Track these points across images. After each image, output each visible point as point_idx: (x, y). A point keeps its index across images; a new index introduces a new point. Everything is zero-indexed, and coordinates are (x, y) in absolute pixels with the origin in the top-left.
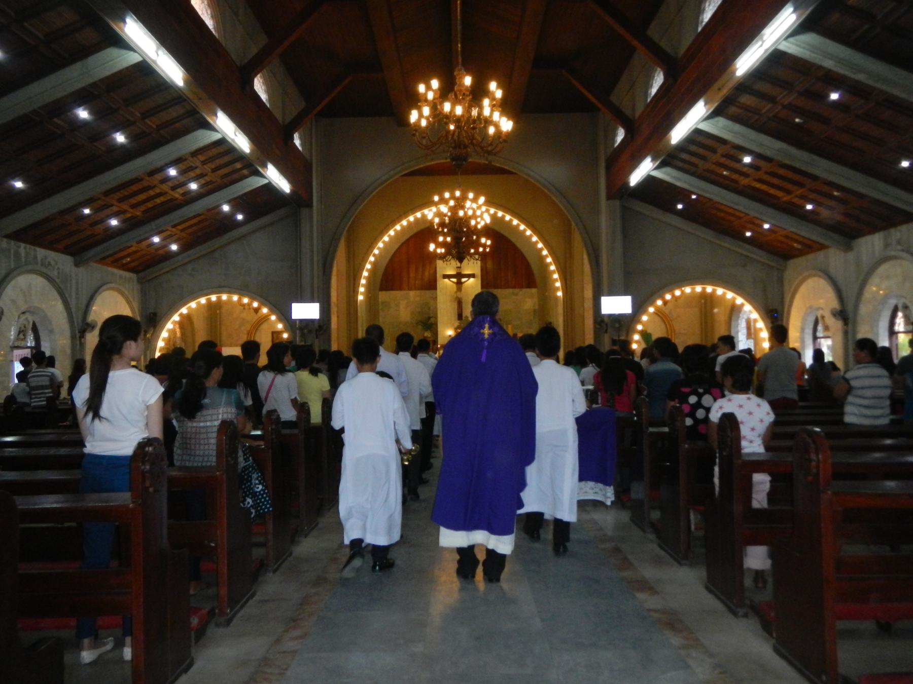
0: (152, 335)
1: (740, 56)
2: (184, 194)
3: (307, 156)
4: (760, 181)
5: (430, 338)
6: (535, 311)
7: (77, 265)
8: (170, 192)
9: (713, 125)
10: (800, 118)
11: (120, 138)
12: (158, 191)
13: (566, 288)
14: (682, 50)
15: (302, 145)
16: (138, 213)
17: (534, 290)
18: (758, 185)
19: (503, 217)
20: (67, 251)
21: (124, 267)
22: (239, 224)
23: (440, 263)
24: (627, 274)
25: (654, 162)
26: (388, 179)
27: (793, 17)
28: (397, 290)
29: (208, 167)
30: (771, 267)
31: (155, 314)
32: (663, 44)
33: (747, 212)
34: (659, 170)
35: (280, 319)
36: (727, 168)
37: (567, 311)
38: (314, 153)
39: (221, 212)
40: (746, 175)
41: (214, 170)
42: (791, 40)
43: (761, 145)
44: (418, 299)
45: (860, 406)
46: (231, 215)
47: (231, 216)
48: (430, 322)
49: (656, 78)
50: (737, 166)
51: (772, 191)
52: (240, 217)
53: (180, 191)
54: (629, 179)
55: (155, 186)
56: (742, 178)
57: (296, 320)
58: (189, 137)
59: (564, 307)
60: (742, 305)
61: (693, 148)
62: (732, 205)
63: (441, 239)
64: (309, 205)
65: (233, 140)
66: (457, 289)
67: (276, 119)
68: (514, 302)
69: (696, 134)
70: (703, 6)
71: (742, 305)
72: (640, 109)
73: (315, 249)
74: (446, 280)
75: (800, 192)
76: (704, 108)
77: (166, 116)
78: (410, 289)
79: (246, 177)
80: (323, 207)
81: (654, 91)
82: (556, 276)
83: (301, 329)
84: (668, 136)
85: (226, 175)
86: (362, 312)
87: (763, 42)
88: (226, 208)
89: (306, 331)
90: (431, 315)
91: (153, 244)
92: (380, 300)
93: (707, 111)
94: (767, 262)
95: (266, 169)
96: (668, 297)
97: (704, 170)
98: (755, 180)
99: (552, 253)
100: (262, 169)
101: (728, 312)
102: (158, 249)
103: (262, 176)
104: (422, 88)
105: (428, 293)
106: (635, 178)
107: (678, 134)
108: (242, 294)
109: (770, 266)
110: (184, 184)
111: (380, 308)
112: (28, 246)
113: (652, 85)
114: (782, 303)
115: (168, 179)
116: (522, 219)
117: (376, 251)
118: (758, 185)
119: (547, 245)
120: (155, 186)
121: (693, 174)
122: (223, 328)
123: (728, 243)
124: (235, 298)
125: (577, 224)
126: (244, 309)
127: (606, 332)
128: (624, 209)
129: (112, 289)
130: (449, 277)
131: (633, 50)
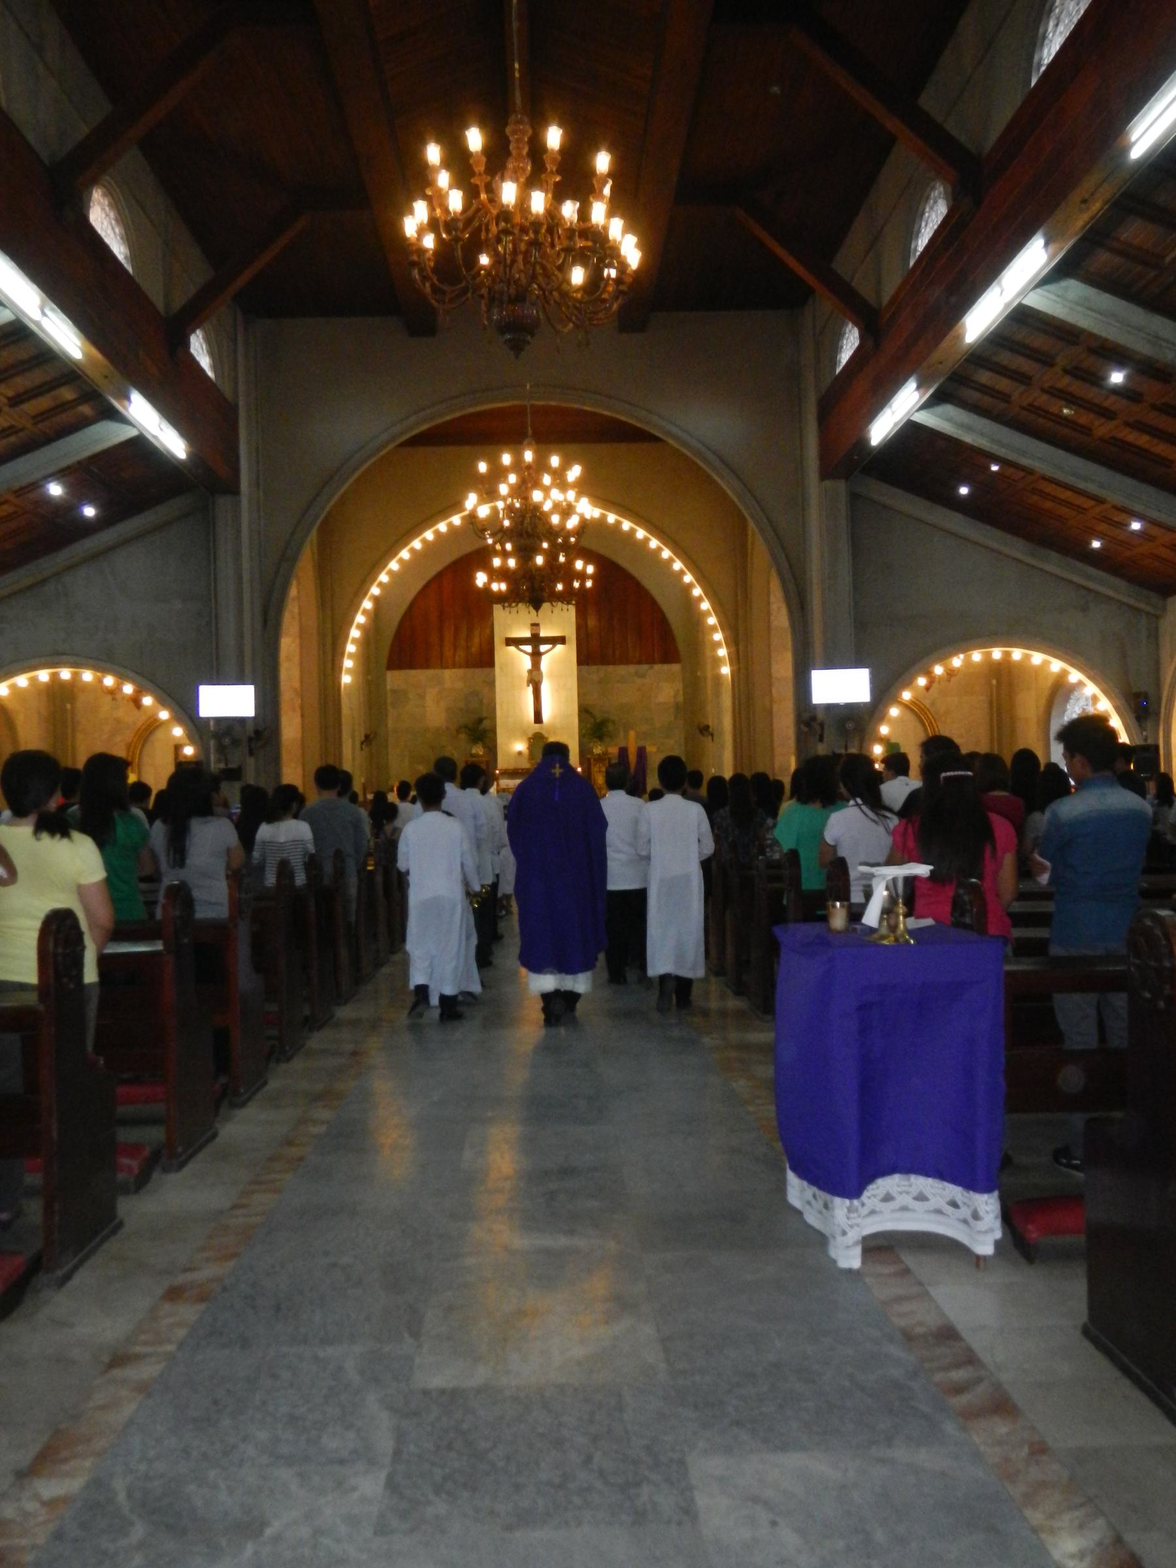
1: (1146, 107)
4: (1139, 426)
5: (481, 756)
6: (677, 706)
9: (1058, 296)
13: (737, 658)
14: (994, 135)
15: (214, 367)
17: (676, 668)
18: (1132, 437)
22: (89, 528)
23: (500, 614)
24: (861, 625)
25: (922, 390)
28: (421, 667)
30: (1138, 610)
32: (951, 127)
33: (1101, 493)
35: (177, 719)
37: (740, 704)
38: (242, 388)
39: (48, 500)
43: (1156, 339)
44: (459, 685)
47: (65, 511)
49: (927, 214)
50: (1091, 393)
52: (89, 512)
54: (869, 431)
56: (1103, 420)
57: (208, 719)
60: (1080, 684)
61: (1005, 358)
62: (1071, 480)
63: (497, 562)
64: (233, 489)
65: (38, 324)
67: (151, 303)
68: (639, 690)
69: (1021, 316)
70: (1041, 30)
71: (1080, 684)
72: (891, 285)
73: (246, 577)
74: (512, 649)
76: (1043, 251)
78: (443, 665)
80: (261, 494)
81: (922, 242)
82: (718, 636)
83: (218, 736)
84: (960, 323)
86: (351, 709)
88: (55, 490)
89: (227, 740)
90: (484, 715)
92: (388, 687)
93: (1050, 259)
94: (1132, 602)
95: (126, 403)
96: (938, 670)
97: (1023, 408)
98: (1127, 424)
99: (711, 592)
100: (117, 402)
101: (1043, 702)
103: (123, 420)
105: (480, 673)
106: (880, 430)
109: (1130, 607)
111: (389, 701)
113: (919, 231)
114: (1158, 685)
116: (655, 529)
117: (375, 591)
119: (702, 578)
122: (80, 737)
123: (1053, 564)
125: (761, 530)
127: (821, 739)
128: (854, 497)
131: (887, 143)
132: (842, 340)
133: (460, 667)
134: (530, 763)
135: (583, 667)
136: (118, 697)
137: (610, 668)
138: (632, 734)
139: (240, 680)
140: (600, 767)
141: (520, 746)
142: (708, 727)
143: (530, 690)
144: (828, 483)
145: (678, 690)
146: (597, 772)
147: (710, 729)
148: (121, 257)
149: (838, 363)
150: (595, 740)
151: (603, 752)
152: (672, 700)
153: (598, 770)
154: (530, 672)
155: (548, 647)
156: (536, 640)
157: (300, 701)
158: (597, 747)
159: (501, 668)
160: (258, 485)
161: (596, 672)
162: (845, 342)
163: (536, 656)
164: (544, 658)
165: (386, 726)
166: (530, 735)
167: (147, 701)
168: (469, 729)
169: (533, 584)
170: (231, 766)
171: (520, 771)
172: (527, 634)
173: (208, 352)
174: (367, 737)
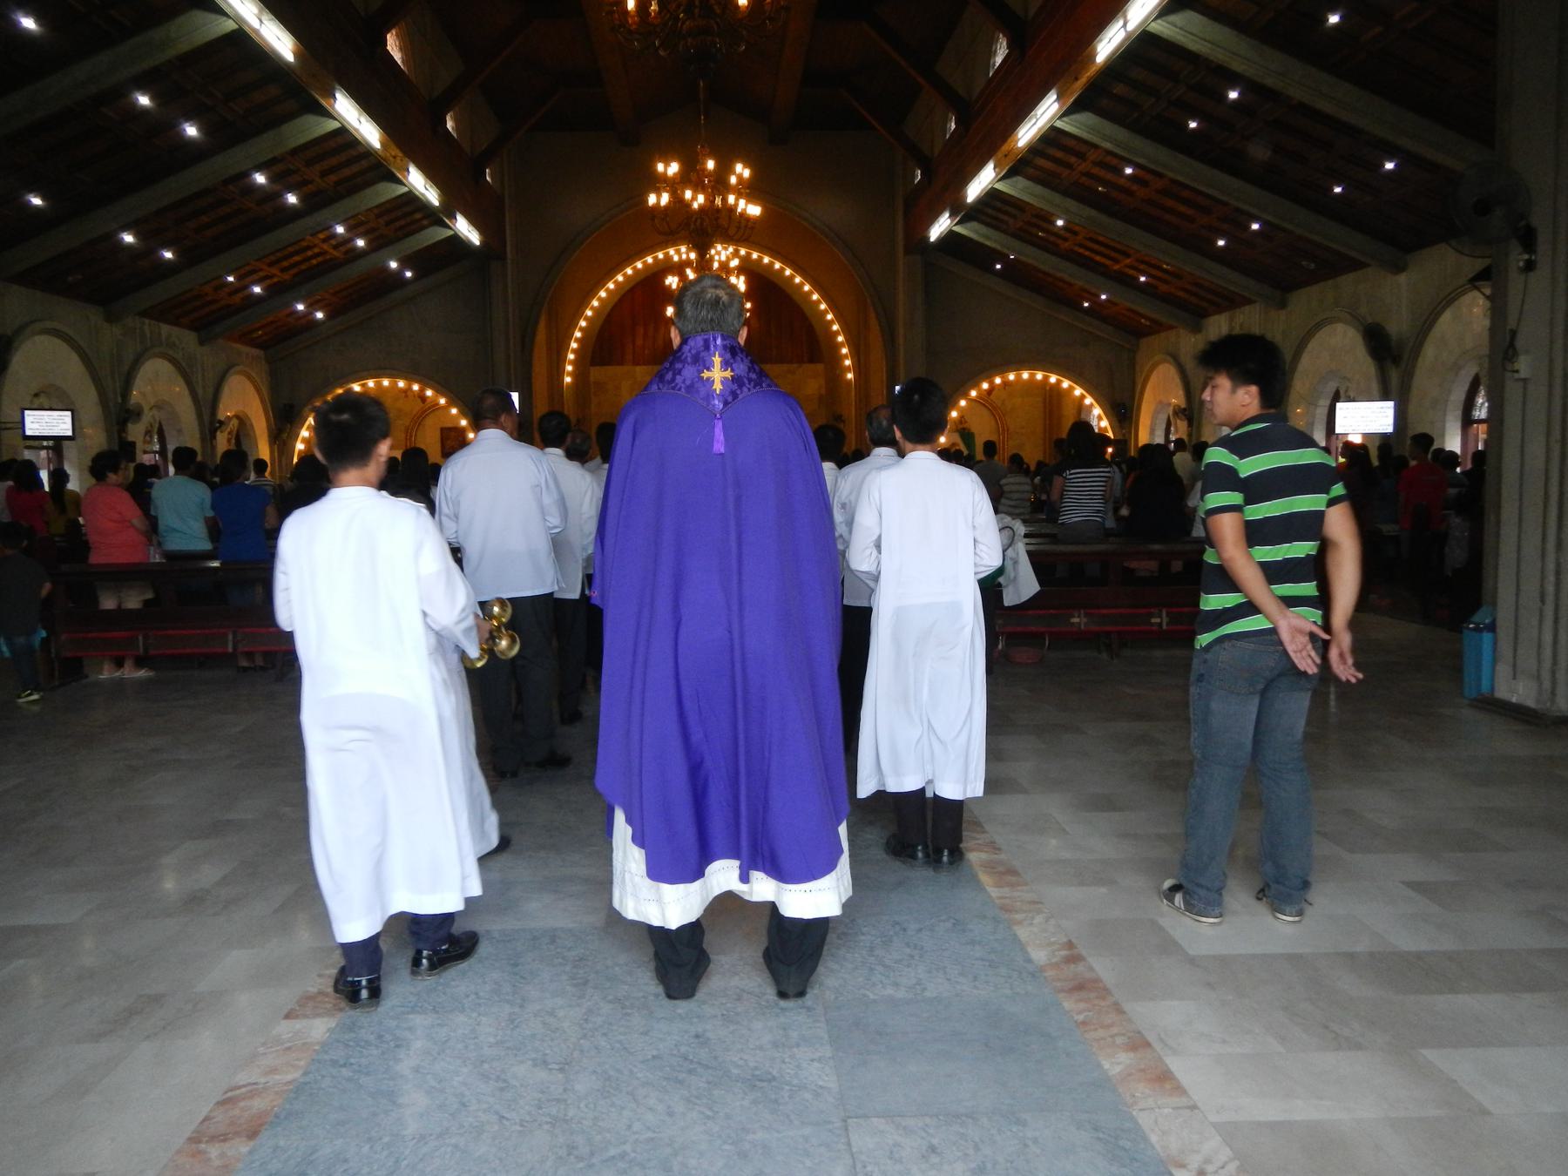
0: (287, 437)
2: (346, 253)
4: (1081, 246)
7: (201, 343)
8: (331, 251)
10: (1104, 187)
11: (292, 199)
12: (316, 250)
13: (859, 368)
16: (287, 276)
17: (820, 367)
18: (1081, 251)
19: (772, 264)
20: (195, 327)
21: (253, 343)
22: (405, 282)
27: (1056, 106)
29: (381, 221)
31: (292, 407)
34: (964, 225)
36: (1043, 230)
40: (1066, 240)
41: (387, 224)
42: (1065, 119)
45: (1010, 506)
46: (400, 272)
50: (1051, 227)
51: (1098, 258)
52: (409, 274)
53: (343, 249)
55: (315, 246)
58: (368, 191)
64: (502, 257)
75: (1128, 261)
77: (347, 172)
78: (636, 363)
79: (424, 228)
85: (401, 228)
87: (1037, 120)
88: (394, 265)
91: (296, 312)
92: (592, 379)
93: (997, 175)
95: (454, 221)
99: (840, 317)
102: (300, 318)
104: (660, 167)
106: (936, 231)
107: (974, 190)
108: (410, 379)
110: (351, 240)
112: (153, 322)
114: (1133, 398)
115: (335, 236)
118: (1081, 251)
120: (315, 246)
121: (1005, 232)
124: (386, 383)
126: (406, 396)
129: (239, 373)
136: (409, 393)
142: (841, 416)
148: (450, 129)
167: (429, 393)
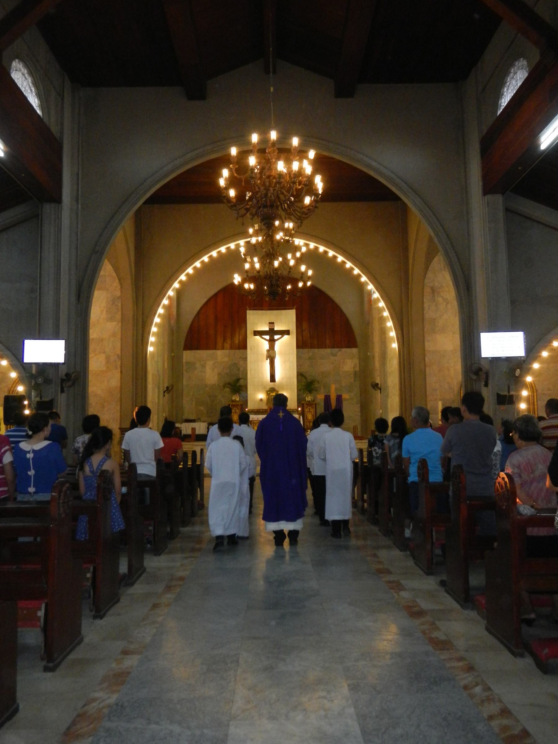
3: (54, 129)
5: (238, 401)
6: (355, 373)
15: (42, 107)
17: (354, 350)
26: (173, 171)
28: (203, 349)
48: (238, 384)
57: (31, 364)
59: (400, 362)
64: (58, 200)
66: (270, 347)
68: (332, 363)
74: (258, 337)
78: (215, 348)
80: (80, 206)
89: (40, 380)
90: (241, 377)
92: (184, 361)
111: (185, 368)
127: (486, 385)
128: (507, 210)
130: (260, 333)
132: (504, 89)
133: (227, 349)
134: (268, 406)
135: (299, 349)
137: (316, 350)
138: (333, 387)
139: (56, 336)
140: (310, 409)
141: (262, 396)
142: (378, 384)
143: (267, 363)
144: (489, 197)
145: (356, 364)
146: (308, 412)
147: (379, 386)
149: (499, 107)
150: (307, 392)
151: (312, 400)
152: (352, 370)
153: (309, 411)
154: (268, 351)
155: (281, 336)
156: (272, 332)
157: (120, 363)
158: (308, 397)
159: (251, 349)
160: (77, 200)
161: (307, 353)
162: (505, 89)
163: (272, 341)
164: (276, 342)
165: (182, 383)
166: (268, 389)
168: (231, 385)
169: (271, 281)
170: (44, 399)
171: (261, 411)
172: (267, 329)
173: (36, 94)
174: (167, 388)
